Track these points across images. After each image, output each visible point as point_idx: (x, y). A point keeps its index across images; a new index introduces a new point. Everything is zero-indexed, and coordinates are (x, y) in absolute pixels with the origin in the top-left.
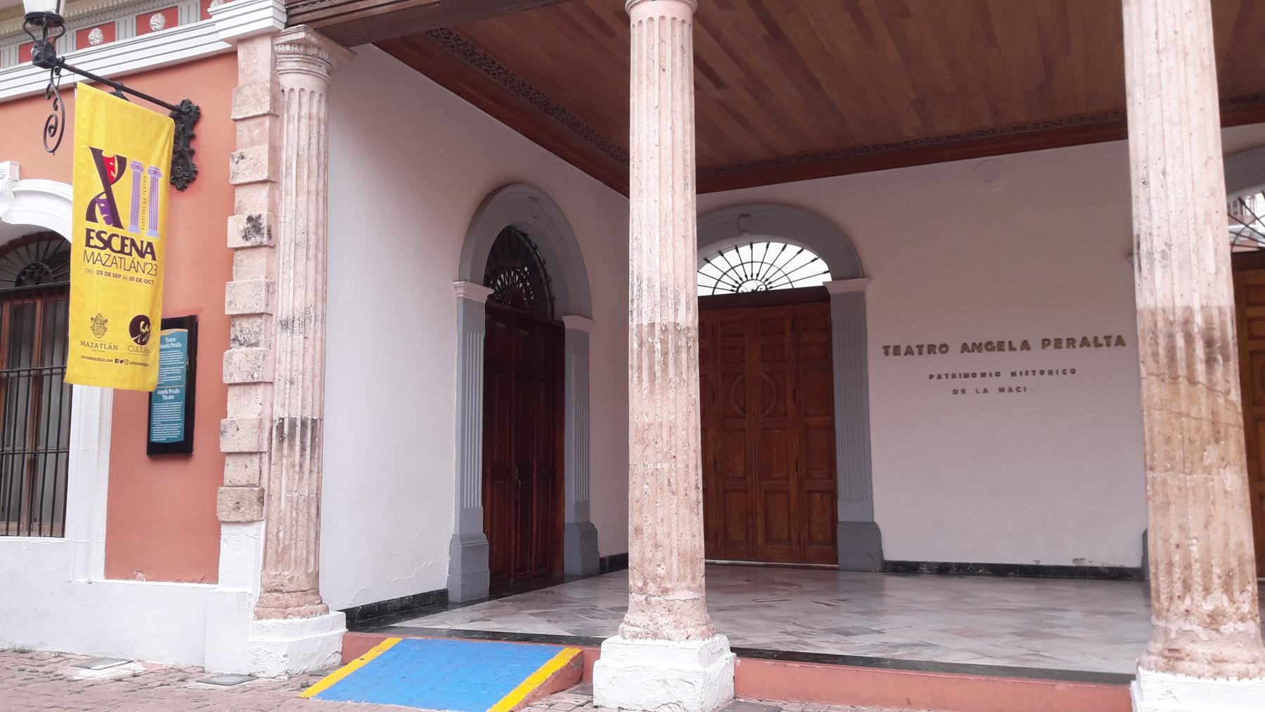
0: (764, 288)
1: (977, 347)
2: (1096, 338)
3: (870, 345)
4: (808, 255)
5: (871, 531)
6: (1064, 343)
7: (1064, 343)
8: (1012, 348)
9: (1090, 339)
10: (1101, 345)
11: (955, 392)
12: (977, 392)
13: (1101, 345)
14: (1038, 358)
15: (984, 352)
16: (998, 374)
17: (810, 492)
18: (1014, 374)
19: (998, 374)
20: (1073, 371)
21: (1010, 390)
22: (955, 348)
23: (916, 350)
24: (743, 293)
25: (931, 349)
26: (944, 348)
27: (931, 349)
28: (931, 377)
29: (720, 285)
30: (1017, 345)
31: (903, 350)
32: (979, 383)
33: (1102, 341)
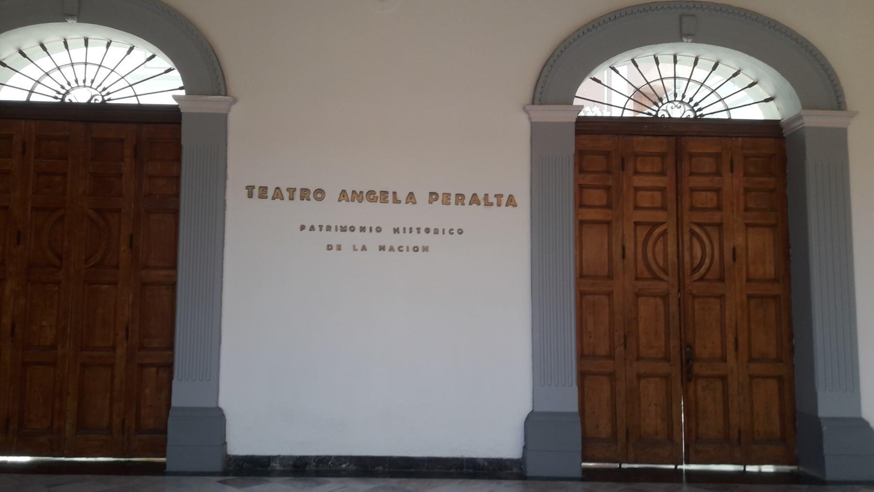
0: (99, 100)
1: (357, 196)
2: (486, 195)
3: (230, 183)
4: (162, 62)
6: (453, 199)
7: (453, 199)
8: (396, 201)
9: (481, 197)
10: (491, 204)
11: (329, 247)
12: (355, 250)
13: (491, 204)
14: (425, 213)
15: (365, 201)
16: (379, 230)
17: (142, 366)
18: (396, 231)
19: (379, 230)
20: (460, 232)
21: (392, 249)
22: (332, 195)
23: (286, 195)
24: (71, 104)
25: (305, 194)
26: (320, 193)
27: (305, 194)
28: (303, 228)
29: (39, 88)
30: (402, 196)
31: (270, 193)
33: (492, 199)
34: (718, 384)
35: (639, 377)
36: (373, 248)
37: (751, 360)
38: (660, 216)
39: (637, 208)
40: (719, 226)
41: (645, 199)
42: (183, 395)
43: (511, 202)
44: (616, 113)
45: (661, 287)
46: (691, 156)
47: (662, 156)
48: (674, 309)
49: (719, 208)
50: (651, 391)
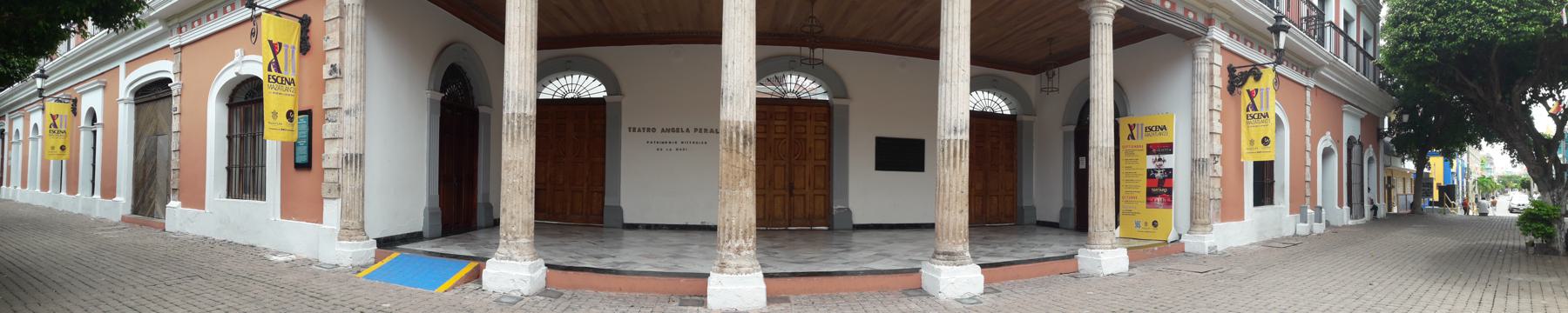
5: (619, 210)
14: (692, 136)
26: (654, 130)
41: (779, 130)
42: (608, 201)
50: (779, 200)
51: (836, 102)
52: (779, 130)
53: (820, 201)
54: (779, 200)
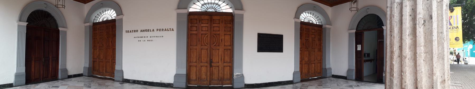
32: (144, 39)
34: (217, 68)
35: (201, 66)
36: (146, 41)
37: (224, 62)
38: (207, 32)
39: (202, 31)
40: (219, 34)
41: (204, 29)
43: (173, 30)
44: (199, 10)
45: (206, 47)
46: (214, 20)
47: (208, 19)
48: (209, 52)
49: (219, 31)
50: (204, 69)
51: (237, 12)
52: (204, 29)
53: (227, 70)
54: (204, 69)
